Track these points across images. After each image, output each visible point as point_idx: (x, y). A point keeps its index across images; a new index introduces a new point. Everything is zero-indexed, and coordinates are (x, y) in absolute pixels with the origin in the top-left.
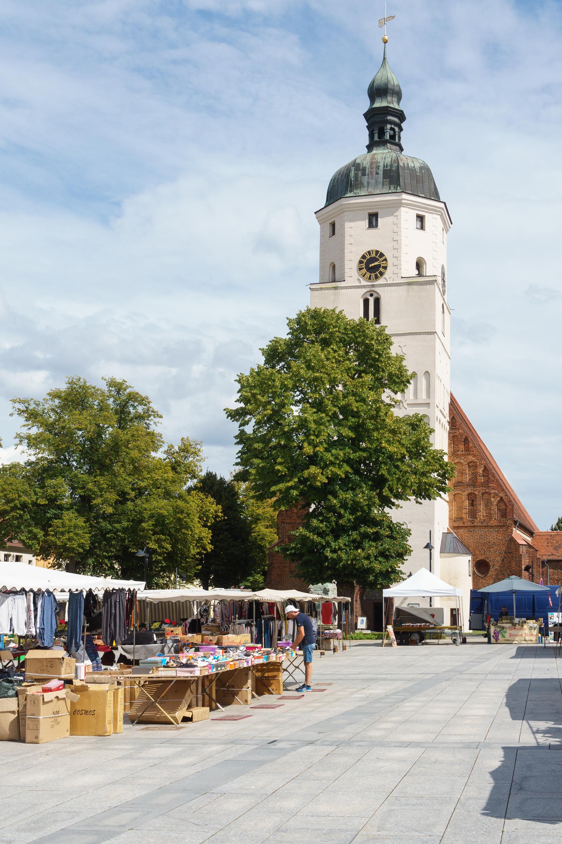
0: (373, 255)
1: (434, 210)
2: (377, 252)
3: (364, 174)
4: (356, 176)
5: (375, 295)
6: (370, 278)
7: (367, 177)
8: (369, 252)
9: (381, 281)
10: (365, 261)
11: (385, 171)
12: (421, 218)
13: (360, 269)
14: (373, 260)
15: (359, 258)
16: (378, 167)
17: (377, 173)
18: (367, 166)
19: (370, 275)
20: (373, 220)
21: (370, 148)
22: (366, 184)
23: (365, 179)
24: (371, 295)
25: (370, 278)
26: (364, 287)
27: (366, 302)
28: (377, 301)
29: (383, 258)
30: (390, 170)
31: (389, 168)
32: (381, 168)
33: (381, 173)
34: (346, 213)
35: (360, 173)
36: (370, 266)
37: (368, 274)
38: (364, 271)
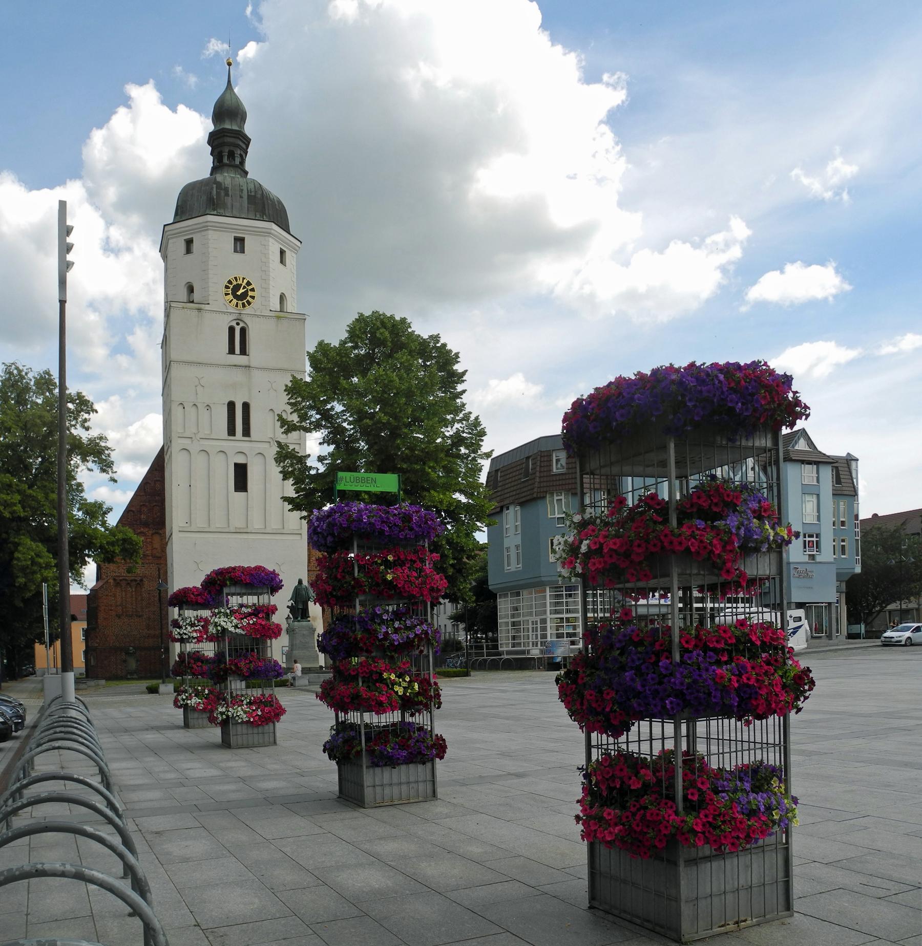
3: (227, 195)
4: (218, 194)
5: (242, 324)
6: (237, 306)
7: (230, 198)
8: (236, 278)
9: (248, 310)
10: (231, 287)
11: (249, 196)
13: (226, 294)
14: (237, 287)
16: (242, 190)
17: (241, 197)
18: (230, 187)
20: (239, 243)
21: (214, 170)
22: (229, 206)
23: (228, 200)
24: (238, 324)
25: (237, 306)
26: (231, 313)
27: (232, 330)
28: (243, 331)
29: (250, 287)
30: (255, 196)
31: (253, 194)
32: (245, 192)
33: (245, 197)
34: (210, 232)
35: (223, 193)
36: (239, 293)
37: (235, 301)
38: (231, 297)
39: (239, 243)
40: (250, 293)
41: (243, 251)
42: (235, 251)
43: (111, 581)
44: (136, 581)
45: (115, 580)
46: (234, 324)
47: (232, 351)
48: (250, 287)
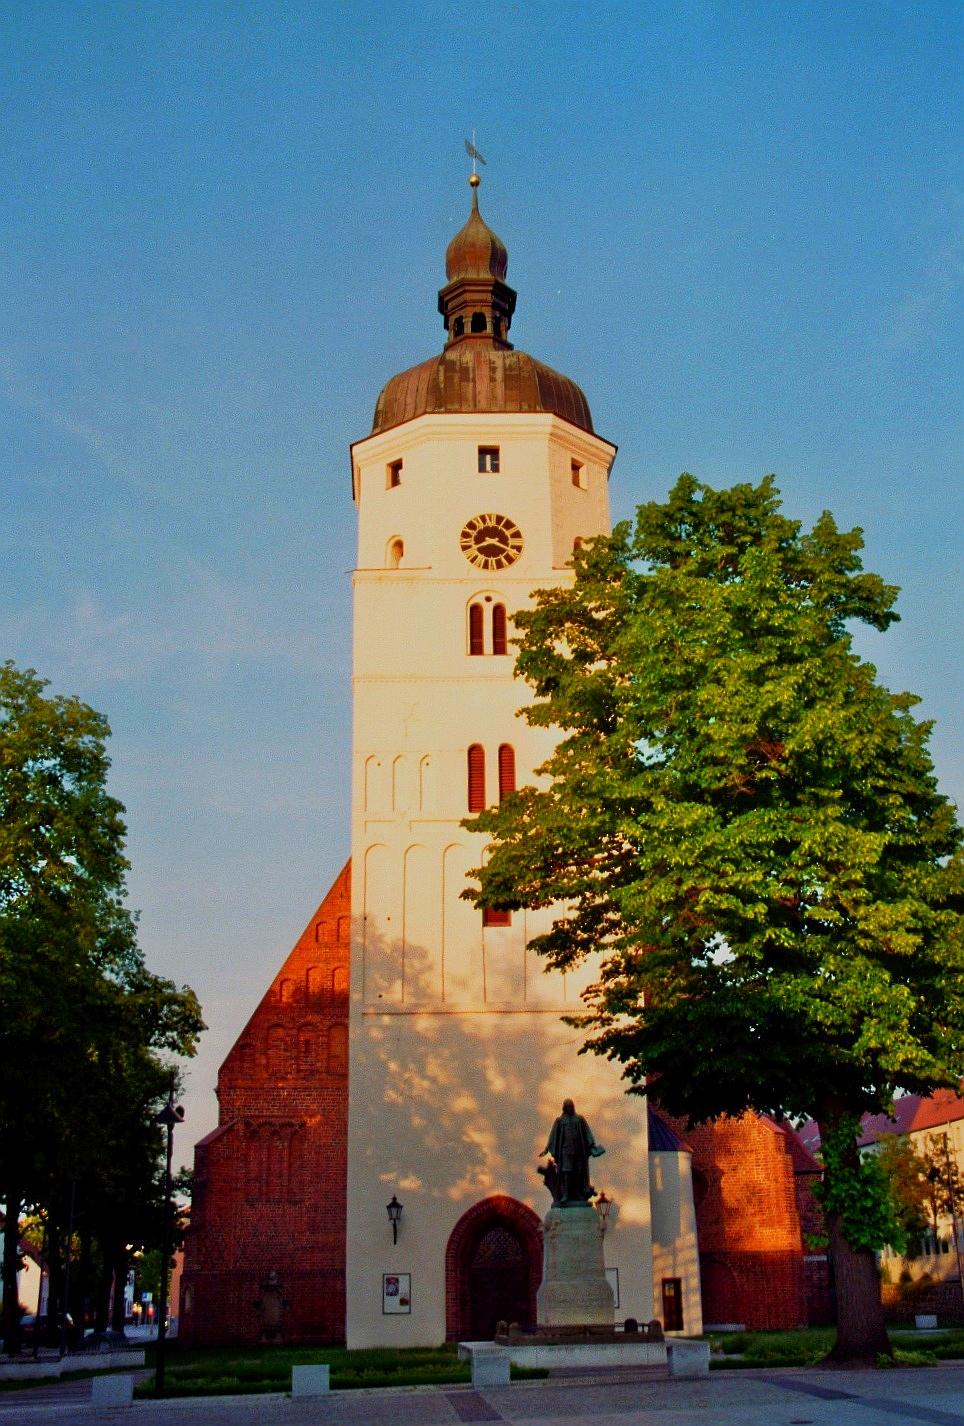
0: (491, 523)
1: (595, 456)
2: (499, 519)
8: (483, 518)
9: (509, 571)
12: (575, 467)
15: (462, 526)
19: (486, 562)
20: (489, 455)
24: (488, 599)
25: (486, 566)
27: (476, 612)
29: (512, 531)
39: (489, 455)
40: (512, 542)
41: (495, 468)
42: (482, 469)
43: (241, 1127)
44: (291, 1125)
45: (247, 1125)
46: (480, 600)
47: (476, 648)
48: (512, 531)
